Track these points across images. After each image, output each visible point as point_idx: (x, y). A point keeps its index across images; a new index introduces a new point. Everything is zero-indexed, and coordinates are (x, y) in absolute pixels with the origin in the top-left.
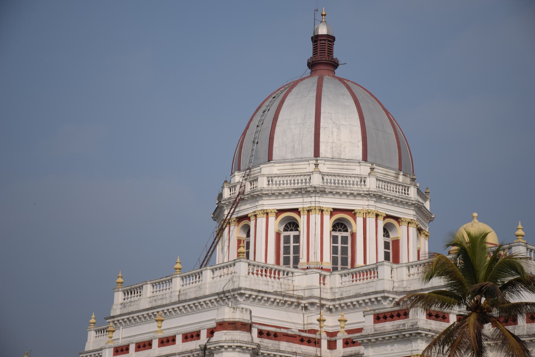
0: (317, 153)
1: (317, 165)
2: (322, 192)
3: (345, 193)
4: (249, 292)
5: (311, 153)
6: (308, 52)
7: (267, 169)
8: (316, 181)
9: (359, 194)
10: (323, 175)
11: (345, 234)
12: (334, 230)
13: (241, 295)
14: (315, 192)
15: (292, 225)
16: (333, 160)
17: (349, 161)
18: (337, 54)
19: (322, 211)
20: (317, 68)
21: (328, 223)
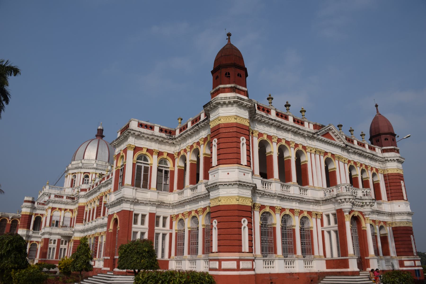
0: (83, 158)
1: (81, 161)
2: (81, 168)
3: (87, 168)
4: (47, 194)
5: (82, 158)
6: (96, 133)
7: (73, 163)
8: (80, 165)
9: (91, 168)
10: (83, 164)
11: (88, 179)
12: (85, 178)
13: (45, 194)
14: (79, 168)
15: (75, 176)
16: (87, 160)
17: (92, 160)
18: (104, 134)
19: (81, 173)
20: (97, 137)
21: (83, 176)
